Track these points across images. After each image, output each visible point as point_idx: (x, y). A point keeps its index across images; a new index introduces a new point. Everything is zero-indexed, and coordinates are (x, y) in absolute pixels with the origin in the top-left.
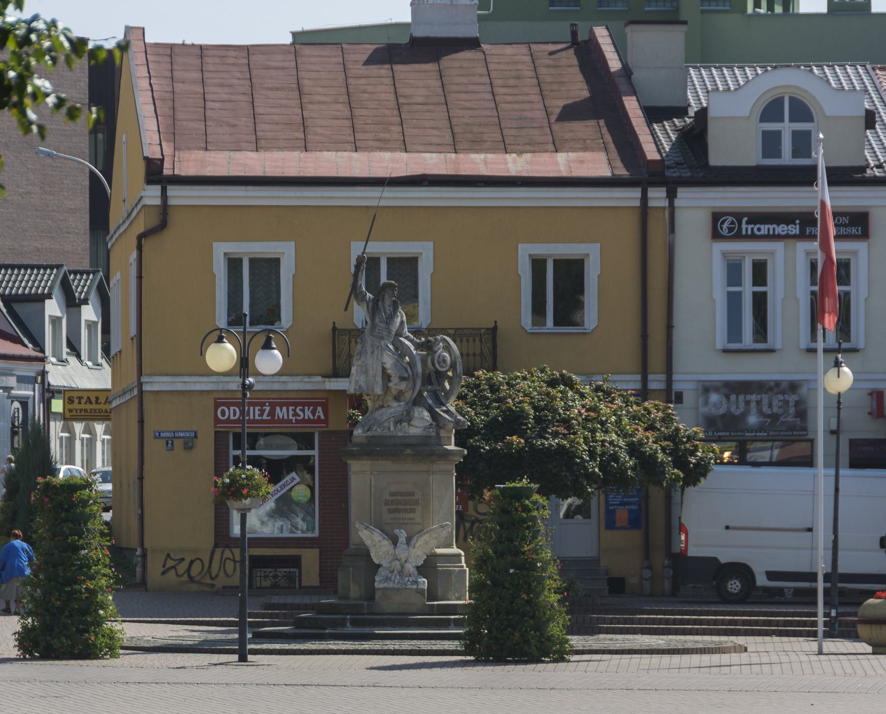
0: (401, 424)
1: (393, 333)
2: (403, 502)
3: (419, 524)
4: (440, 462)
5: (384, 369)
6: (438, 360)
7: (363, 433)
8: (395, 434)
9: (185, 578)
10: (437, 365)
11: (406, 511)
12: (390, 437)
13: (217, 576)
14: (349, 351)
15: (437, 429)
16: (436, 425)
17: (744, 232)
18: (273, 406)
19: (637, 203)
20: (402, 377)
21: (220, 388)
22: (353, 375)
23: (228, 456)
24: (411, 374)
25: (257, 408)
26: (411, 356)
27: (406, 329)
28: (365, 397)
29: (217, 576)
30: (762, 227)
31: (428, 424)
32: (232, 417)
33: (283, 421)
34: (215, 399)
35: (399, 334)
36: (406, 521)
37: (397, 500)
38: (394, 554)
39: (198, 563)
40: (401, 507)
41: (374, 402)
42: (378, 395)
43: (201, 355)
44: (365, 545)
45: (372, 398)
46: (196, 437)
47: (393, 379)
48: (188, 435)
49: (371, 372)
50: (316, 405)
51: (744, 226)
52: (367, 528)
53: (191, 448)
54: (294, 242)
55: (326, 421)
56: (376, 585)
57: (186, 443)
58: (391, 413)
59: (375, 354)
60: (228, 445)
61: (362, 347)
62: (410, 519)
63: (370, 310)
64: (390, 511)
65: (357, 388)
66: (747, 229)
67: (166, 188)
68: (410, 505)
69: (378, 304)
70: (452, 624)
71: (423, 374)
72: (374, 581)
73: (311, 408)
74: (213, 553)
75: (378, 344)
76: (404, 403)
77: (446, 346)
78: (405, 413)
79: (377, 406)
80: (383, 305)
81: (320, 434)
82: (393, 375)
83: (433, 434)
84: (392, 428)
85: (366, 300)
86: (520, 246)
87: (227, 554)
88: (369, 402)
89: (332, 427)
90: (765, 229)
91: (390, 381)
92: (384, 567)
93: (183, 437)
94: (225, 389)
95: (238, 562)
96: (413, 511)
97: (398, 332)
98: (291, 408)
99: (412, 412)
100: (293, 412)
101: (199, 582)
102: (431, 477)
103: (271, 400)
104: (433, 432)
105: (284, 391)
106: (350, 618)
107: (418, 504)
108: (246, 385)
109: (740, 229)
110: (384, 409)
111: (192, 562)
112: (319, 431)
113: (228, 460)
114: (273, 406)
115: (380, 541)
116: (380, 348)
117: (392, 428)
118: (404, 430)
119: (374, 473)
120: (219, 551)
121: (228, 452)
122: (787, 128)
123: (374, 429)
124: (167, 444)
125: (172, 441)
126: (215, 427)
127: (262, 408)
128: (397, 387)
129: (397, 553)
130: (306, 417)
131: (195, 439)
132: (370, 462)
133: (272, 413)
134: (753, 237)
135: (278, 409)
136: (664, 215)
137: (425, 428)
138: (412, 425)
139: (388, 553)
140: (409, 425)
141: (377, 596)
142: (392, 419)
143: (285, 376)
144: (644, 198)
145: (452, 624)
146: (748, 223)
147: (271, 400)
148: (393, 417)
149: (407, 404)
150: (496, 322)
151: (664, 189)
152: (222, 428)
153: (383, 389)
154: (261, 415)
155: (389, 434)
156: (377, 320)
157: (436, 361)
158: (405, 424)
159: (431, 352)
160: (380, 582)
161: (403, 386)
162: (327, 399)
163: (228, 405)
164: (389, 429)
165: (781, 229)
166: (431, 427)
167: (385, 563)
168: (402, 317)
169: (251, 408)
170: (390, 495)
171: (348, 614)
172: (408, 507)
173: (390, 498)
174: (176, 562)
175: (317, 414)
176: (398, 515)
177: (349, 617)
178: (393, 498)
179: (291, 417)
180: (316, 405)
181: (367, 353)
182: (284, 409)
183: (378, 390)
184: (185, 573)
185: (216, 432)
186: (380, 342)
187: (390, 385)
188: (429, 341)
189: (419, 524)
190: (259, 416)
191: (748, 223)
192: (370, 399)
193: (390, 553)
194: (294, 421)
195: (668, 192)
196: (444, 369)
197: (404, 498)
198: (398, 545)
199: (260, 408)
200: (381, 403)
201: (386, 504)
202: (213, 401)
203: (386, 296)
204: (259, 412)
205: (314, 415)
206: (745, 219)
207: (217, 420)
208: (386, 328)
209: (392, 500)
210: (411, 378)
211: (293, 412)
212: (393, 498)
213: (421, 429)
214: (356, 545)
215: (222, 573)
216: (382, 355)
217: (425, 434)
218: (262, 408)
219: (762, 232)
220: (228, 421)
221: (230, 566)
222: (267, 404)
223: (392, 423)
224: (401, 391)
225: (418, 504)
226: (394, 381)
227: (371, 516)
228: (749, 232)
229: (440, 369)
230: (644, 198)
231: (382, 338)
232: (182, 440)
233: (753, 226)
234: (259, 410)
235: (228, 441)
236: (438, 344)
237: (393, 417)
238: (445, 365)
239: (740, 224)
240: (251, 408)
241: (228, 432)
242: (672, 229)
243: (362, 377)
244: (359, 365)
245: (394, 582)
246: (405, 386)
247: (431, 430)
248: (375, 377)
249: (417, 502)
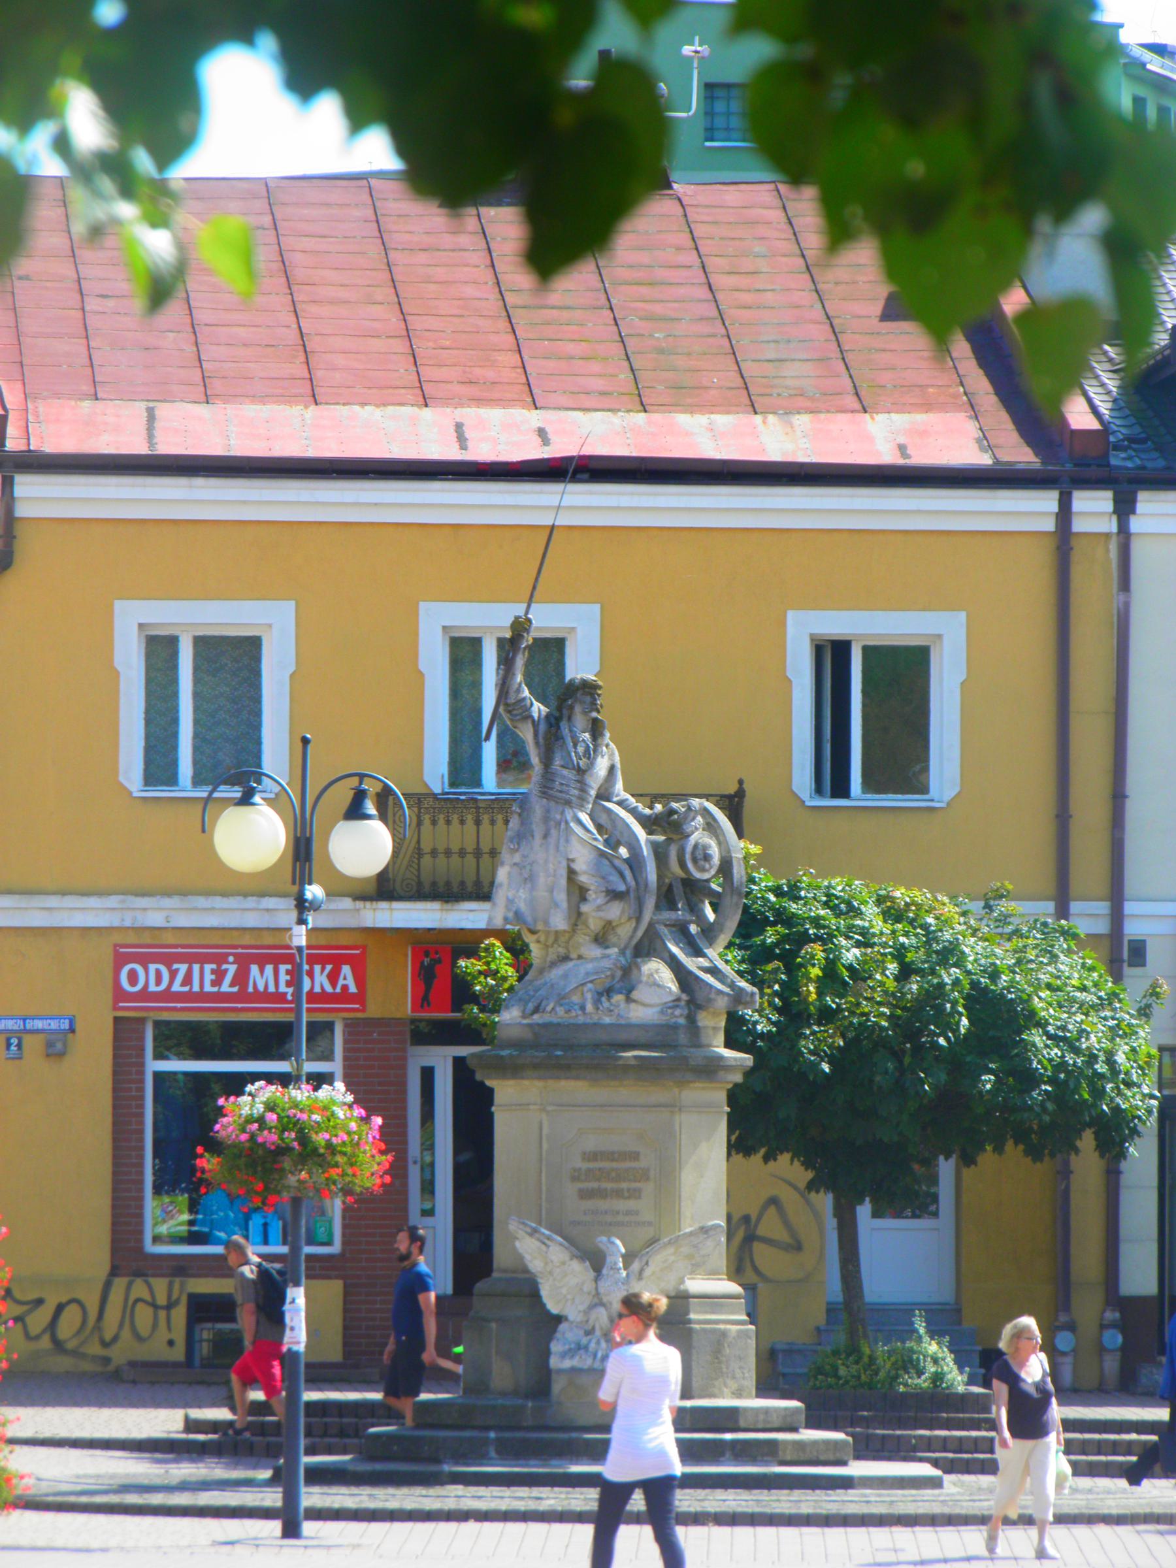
0: (609, 998)
1: (593, 793)
2: (613, 1174)
3: (650, 1224)
4: (697, 1084)
5: (571, 873)
6: (693, 853)
7: (524, 1017)
8: (595, 1019)
9: (45, 1343)
10: (690, 865)
11: (618, 1194)
12: (585, 1026)
13: (115, 1338)
14: (418, 842)
15: (689, 1009)
16: (689, 1002)
18: (244, 963)
19: (1049, 525)
20: (613, 891)
21: (128, 923)
22: (501, 885)
23: (142, 1073)
24: (633, 883)
25: (208, 968)
26: (634, 846)
27: (619, 785)
28: (528, 938)
29: (115, 1338)
31: (671, 998)
32: (153, 988)
33: (265, 996)
34: (115, 946)
35: (604, 794)
36: (620, 1218)
37: (600, 1169)
38: (594, 1292)
39: (72, 1313)
40: (609, 1186)
41: (547, 946)
42: (557, 932)
43: (203, 831)
44: (526, 1270)
45: (542, 939)
46: (72, 1030)
47: (591, 895)
48: (54, 1025)
49: (542, 880)
50: (337, 962)
52: (534, 1232)
53: (61, 1055)
54: (293, 603)
55: (360, 998)
56: (554, 1362)
57: (49, 1044)
58: (587, 974)
59: (552, 840)
60: (142, 1049)
61: (522, 823)
62: (628, 1213)
63: (541, 740)
64: (585, 1195)
65: (511, 915)
67: (12, 478)
68: (630, 1181)
69: (559, 728)
70: (728, 1455)
71: (659, 887)
72: (547, 1353)
73: (329, 967)
74: (107, 1286)
76: (616, 950)
77: (708, 824)
78: (619, 973)
79: (552, 956)
80: (571, 731)
81: (346, 1026)
82: (592, 888)
83: (682, 1021)
84: (589, 1007)
85: (531, 717)
86: (791, 615)
87: (139, 1289)
88: (533, 947)
89: (374, 1009)
91: (584, 899)
92: (572, 1323)
93: (42, 1031)
94: (138, 924)
95: (162, 1308)
96: (635, 1194)
97: (602, 791)
98: (283, 968)
99: (635, 972)
100: (288, 978)
101: (75, 1353)
102: (677, 1118)
103: (240, 951)
104: (681, 1015)
105: (268, 929)
106: (497, 1439)
107: (648, 1179)
108: (306, 900)
110: (570, 964)
111: (60, 1308)
112: (344, 1019)
113: (142, 1081)
114: (244, 963)
115: (564, 1263)
116: (563, 826)
117: (589, 1007)
118: (616, 1011)
119: (550, 1108)
120: (120, 1283)
121: (142, 1065)
123: (549, 1008)
124: (9, 1045)
125: (20, 1039)
126: (115, 1008)
127: (219, 966)
128: (601, 914)
129: (601, 1290)
130: (317, 989)
131: (71, 1035)
132: (539, 1084)
133: (241, 978)
135: (254, 969)
136: (1108, 551)
137: (666, 1008)
138: (634, 1001)
139: (581, 1289)
140: (629, 1000)
141: (557, 1386)
142: (590, 985)
143: (271, 896)
144: (1065, 514)
145: (728, 1455)
147: (240, 951)
148: (591, 982)
149: (622, 952)
150: (741, 782)
151: (1109, 494)
152: (129, 1010)
153: (570, 918)
154: (217, 982)
155: (581, 1019)
156: (558, 761)
157: (688, 857)
158: (619, 998)
159: (675, 837)
160: (563, 1355)
161: (615, 911)
162: (364, 948)
163: (144, 960)
164: (583, 1008)
166: (677, 1006)
167: (573, 1313)
168: (612, 755)
169: (196, 967)
170: (583, 1159)
171: (487, 1428)
172: (624, 1185)
173: (585, 1166)
174: (25, 1308)
175: (341, 982)
176: (603, 1204)
177: (492, 1435)
178: (592, 1165)
179: (283, 988)
180: (337, 962)
181: (533, 836)
182: (269, 969)
183: (559, 922)
184: (44, 1331)
185: (116, 1019)
186: (563, 813)
187: (585, 908)
188: (672, 812)
189: (650, 1224)
190: (214, 983)
192: (538, 941)
193: (585, 1289)
194: (289, 997)
195: (1116, 501)
196: (706, 876)
197: (614, 1165)
198: (605, 1271)
199: (214, 966)
200: (562, 951)
201: (575, 1179)
202: (110, 951)
203: (578, 709)
204: (213, 977)
205: (334, 985)
207: (119, 995)
208: (578, 781)
209: (589, 1170)
210: (632, 895)
211: (288, 978)
212: (592, 1165)
214: (505, 1271)
215: (126, 1334)
216: (567, 841)
217: (663, 1019)
218: (219, 966)
220: (144, 995)
221: (143, 1315)
222: (231, 959)
223: (589, 996)
224: (609, 923)
225: (648, 1179)
226: (595, 900)
227: (540, 1206)
229: (698, 875)
230: (1065, 514)
231: (568, 803)
232: (41, 1036)
234: (213, 972)
235: (142, 1039)
236: (694, 819)
237: (591, 982)
238: (707, 866)
240: (196, 967)
241: (142, 1021)
242: (1125, 583)
243: (521, 891)
244: (515, 864)
245: (595, 1355)
246: (618, 913)
247: (678, 1012)
248: (551, 890)
249: (644, 1176)
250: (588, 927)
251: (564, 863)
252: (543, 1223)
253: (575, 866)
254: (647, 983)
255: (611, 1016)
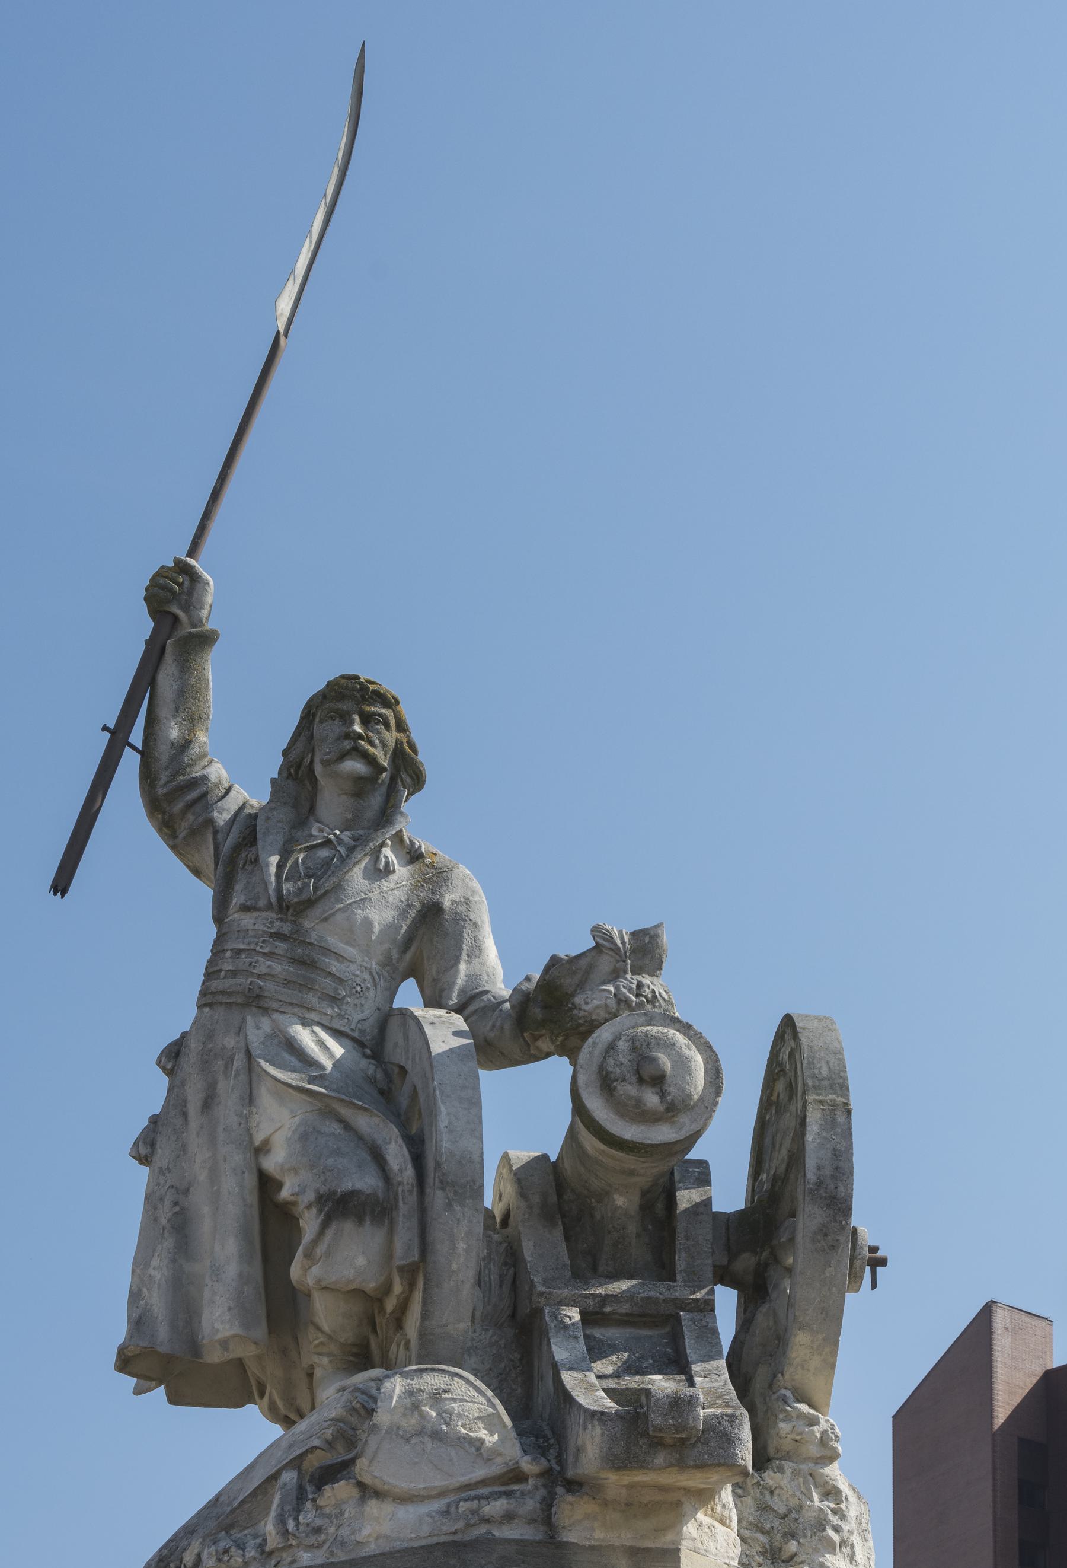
24: (407, 1173)
31: (480, 1473)
75: (230, 1042)
104: (509, 1517)
118: (332, 1530)
186: (240, 1030)
208: (279, 936)
213: (437, 1505)
250: (319, 1329)
251: (237, 1158)
253: (272, 1163)
254: (394, 1431)
255: (319, 1546)
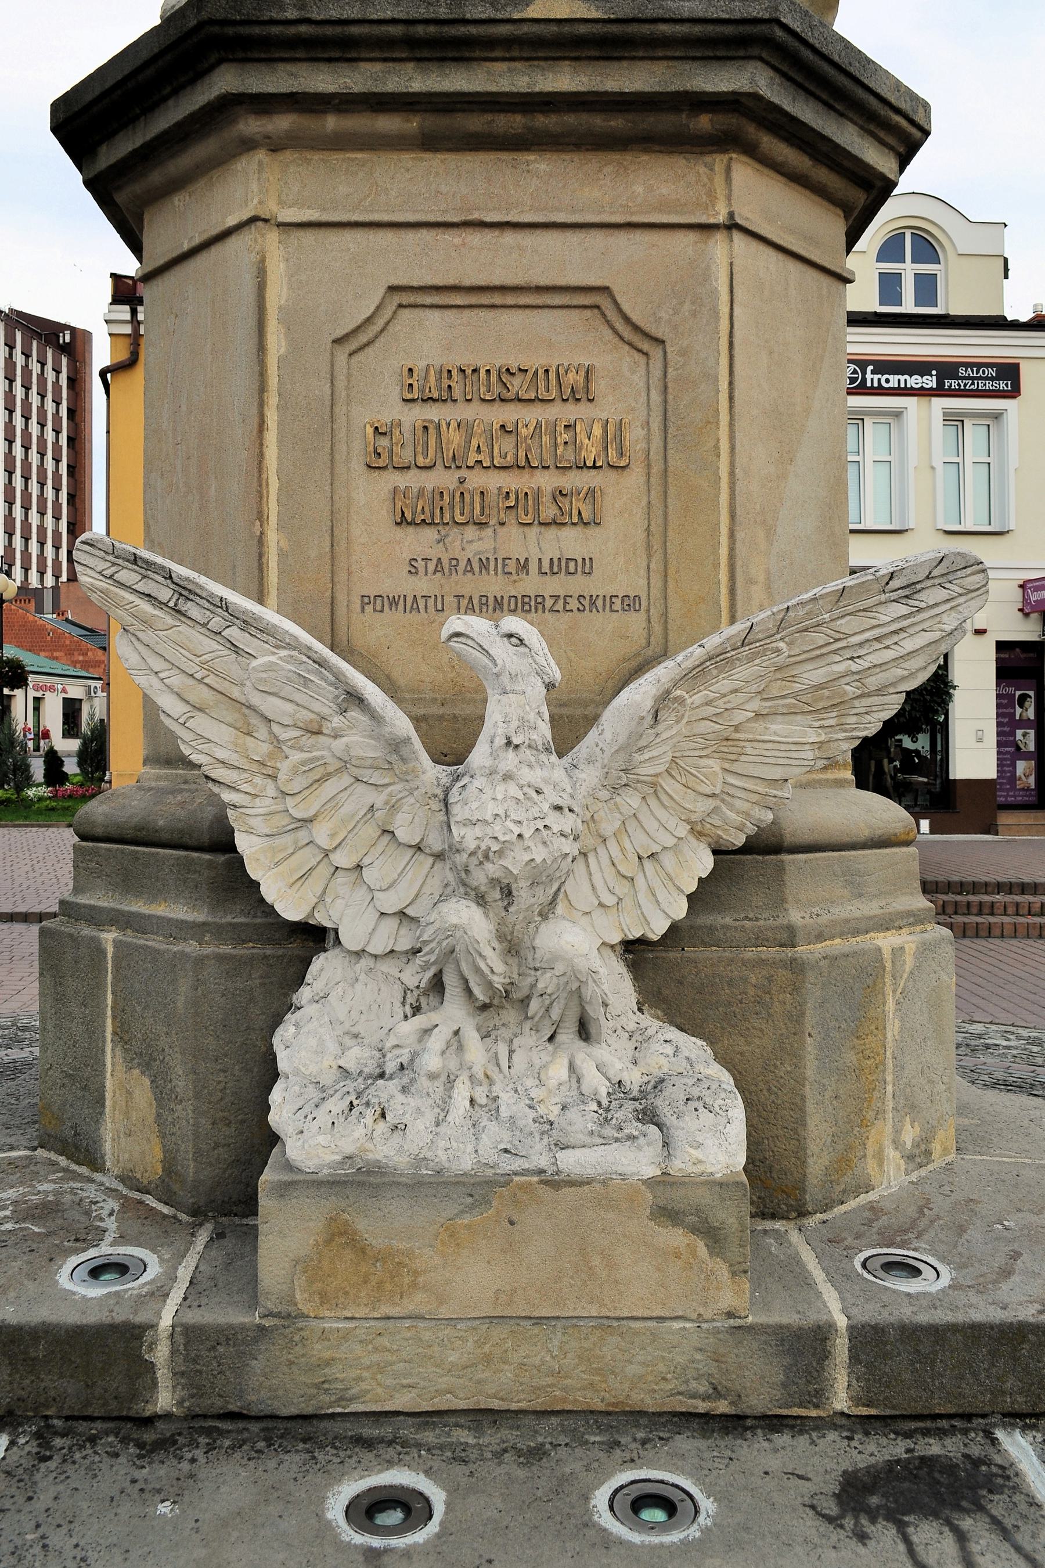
17: (869, 384)
30: (891, 377)
51: (869, 376)
66: (872, 380)
90: (894, 381)
109: (864, 379)
122: (909, 270)
134: (880, 391)
146: (873, 372)
165: (914, 381)
172: (546, 481)
189: (630, 603)
191: (873, 372)
197: (509, 414)
198: (479, 756)
206: (870, 368)
219: (890, 385)
227: (261, 541)
228: (876, 385)
233: (880, 376)
239: (864, 373)
252: (273, 597)
